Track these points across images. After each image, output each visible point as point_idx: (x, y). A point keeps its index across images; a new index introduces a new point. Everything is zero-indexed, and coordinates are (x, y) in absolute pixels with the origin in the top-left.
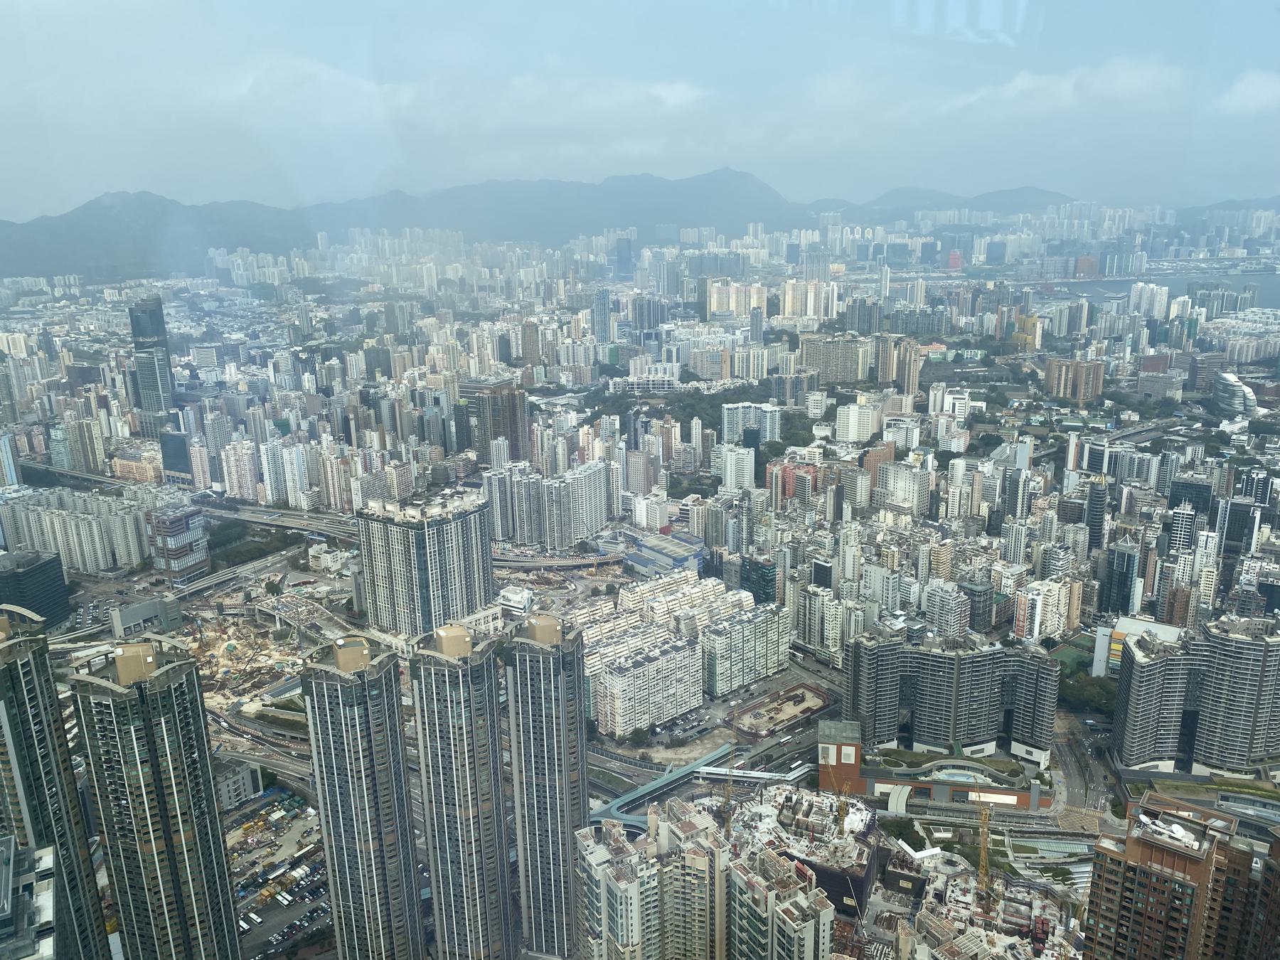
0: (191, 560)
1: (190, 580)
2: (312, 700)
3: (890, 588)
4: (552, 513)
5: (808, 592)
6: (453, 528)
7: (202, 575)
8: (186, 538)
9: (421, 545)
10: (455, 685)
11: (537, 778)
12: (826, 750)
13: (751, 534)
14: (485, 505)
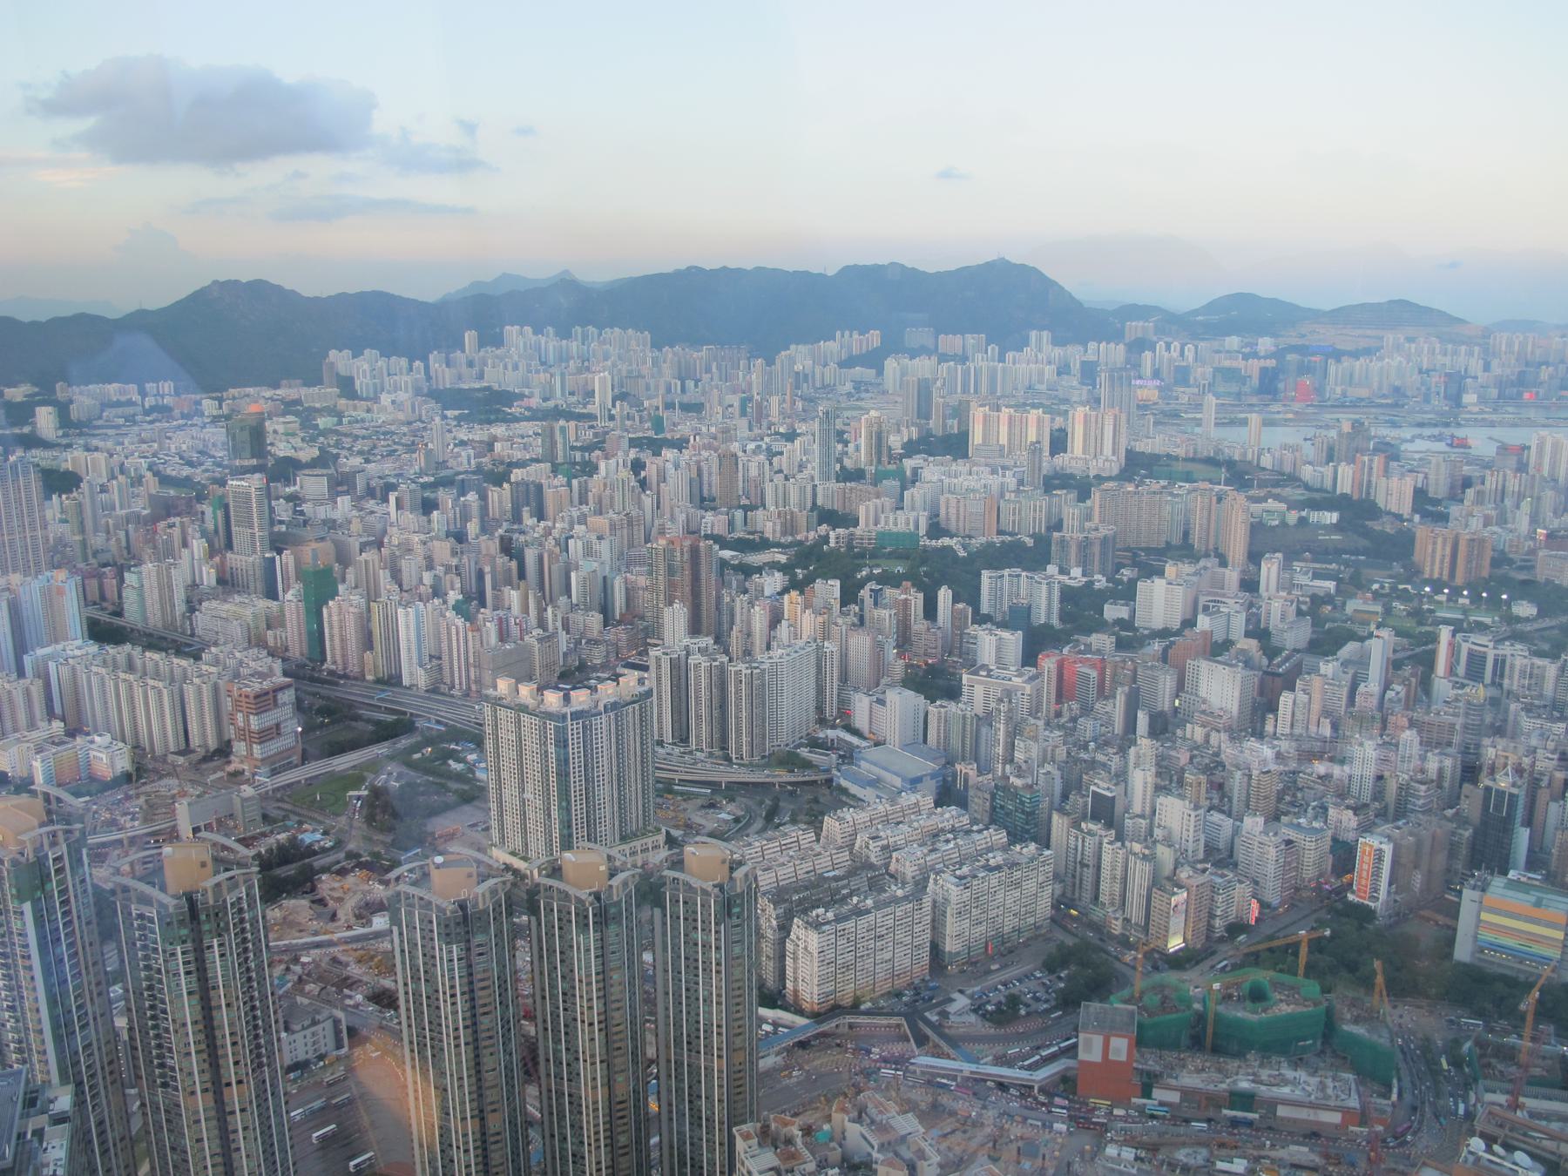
0: (275, 746)
1: (274, 772)
2: (401, 934)
3: (1192, 829)
4: (739, 714)
5: (1082, 831)
6: (602, 723)
7: (290, 766)
8: (269, 719)
9: (562, 743)
11: (689, 1056)
12: (1088, 1044)
13: (1011, 747)
14: (649, 693)
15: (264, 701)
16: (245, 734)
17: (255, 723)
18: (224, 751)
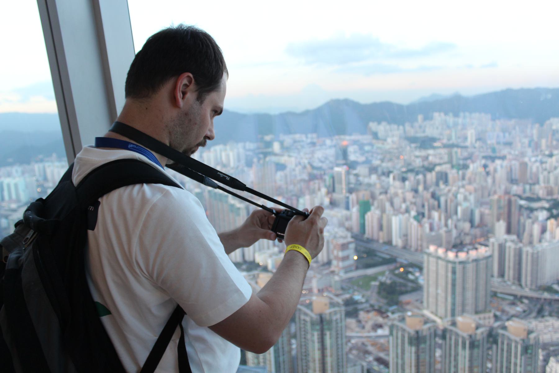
1: (346, 272)
4: (527, 268)
6: (470, 267)
7: (351, 271)
8: (345, 253)
10: (464, 347)
14: (491, 256)
15: (344, 247)
16: (337, 258)
17: (341, 254)
18: (329, 263)
